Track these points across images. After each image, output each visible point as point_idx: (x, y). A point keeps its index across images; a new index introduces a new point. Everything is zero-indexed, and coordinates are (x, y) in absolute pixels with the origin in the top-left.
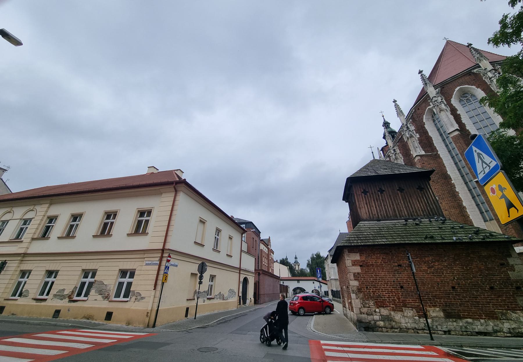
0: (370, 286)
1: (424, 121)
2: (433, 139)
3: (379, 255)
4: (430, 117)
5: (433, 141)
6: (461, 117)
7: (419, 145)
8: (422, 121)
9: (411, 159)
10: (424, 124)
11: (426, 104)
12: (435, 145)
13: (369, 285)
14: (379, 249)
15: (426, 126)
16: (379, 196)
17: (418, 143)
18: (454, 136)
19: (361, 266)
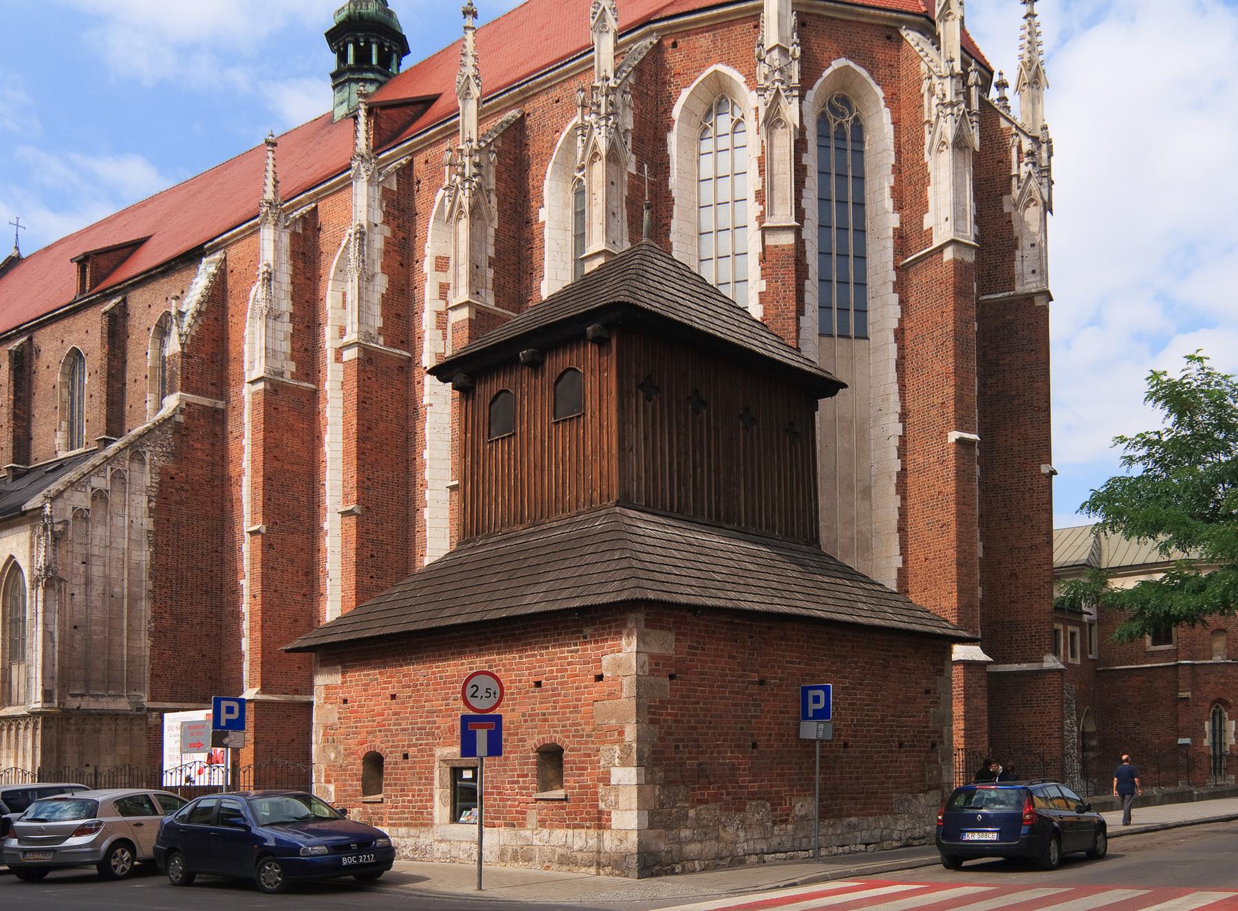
0: (686, 743)
1: (676, 112)
2: (675, 208)
3: (724, 645)
4: (701, 109)
5: (671, 217)
6: (804, 182)
7: (625, 211)
8: (669, 110)
9: (523, 243)
10: (669, 128)
11: (715, 46)
12: (673, 237)
13: (683, 740)
14: (726, 623)
15: (673, 139)
16: (687, 419)
17: (624, 198)
18: (776, 247)
19: (672, 677)
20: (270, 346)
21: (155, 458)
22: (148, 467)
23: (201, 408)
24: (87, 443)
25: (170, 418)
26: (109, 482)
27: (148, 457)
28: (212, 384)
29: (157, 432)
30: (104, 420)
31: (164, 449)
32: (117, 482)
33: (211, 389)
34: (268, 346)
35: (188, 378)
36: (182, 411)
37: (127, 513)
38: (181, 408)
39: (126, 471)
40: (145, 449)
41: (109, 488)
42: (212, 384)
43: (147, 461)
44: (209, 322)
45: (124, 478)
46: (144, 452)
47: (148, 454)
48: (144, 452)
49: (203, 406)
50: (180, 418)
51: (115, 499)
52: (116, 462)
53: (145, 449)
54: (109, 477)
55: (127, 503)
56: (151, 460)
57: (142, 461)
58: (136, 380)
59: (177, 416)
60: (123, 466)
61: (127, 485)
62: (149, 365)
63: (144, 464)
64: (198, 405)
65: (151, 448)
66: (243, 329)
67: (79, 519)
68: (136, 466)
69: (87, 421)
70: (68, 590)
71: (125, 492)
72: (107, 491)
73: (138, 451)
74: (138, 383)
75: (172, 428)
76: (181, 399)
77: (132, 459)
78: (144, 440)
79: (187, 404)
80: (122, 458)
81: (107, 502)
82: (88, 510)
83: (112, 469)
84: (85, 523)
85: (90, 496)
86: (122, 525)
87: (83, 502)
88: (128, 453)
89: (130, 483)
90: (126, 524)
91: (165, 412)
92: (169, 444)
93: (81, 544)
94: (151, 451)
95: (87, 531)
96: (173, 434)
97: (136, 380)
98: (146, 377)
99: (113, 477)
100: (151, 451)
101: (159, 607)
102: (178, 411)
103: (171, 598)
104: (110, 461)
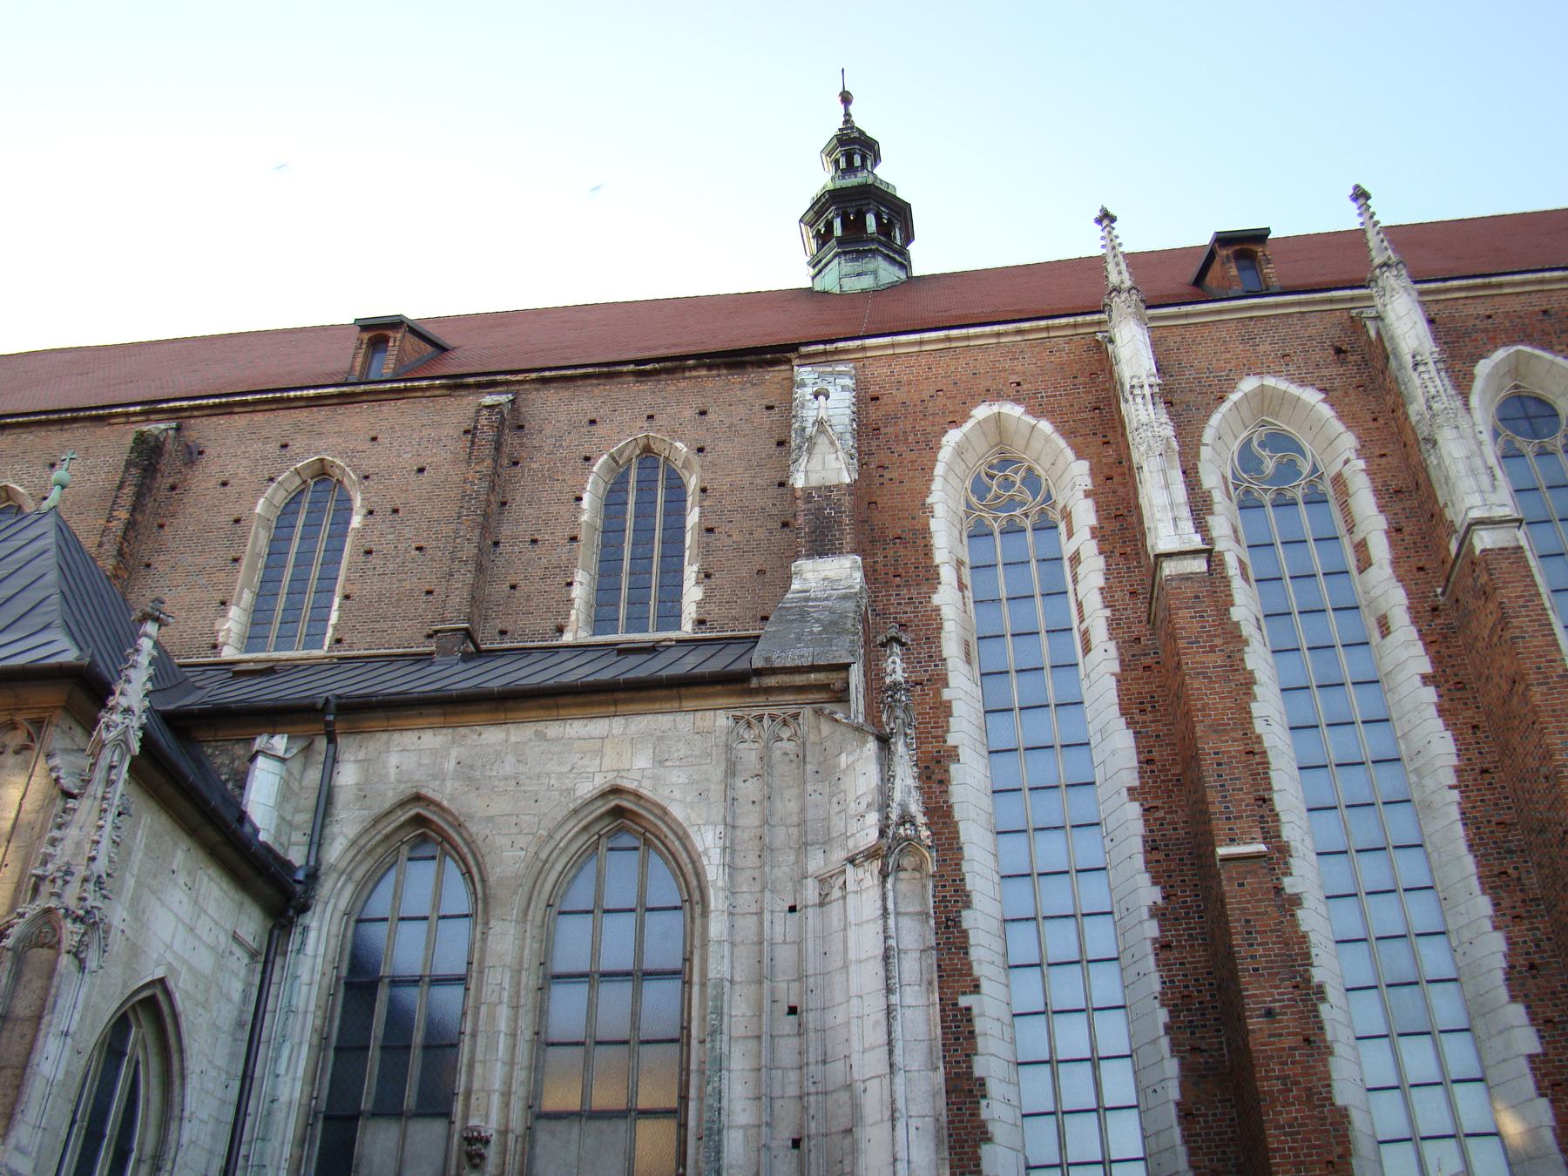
62: (584, 518)
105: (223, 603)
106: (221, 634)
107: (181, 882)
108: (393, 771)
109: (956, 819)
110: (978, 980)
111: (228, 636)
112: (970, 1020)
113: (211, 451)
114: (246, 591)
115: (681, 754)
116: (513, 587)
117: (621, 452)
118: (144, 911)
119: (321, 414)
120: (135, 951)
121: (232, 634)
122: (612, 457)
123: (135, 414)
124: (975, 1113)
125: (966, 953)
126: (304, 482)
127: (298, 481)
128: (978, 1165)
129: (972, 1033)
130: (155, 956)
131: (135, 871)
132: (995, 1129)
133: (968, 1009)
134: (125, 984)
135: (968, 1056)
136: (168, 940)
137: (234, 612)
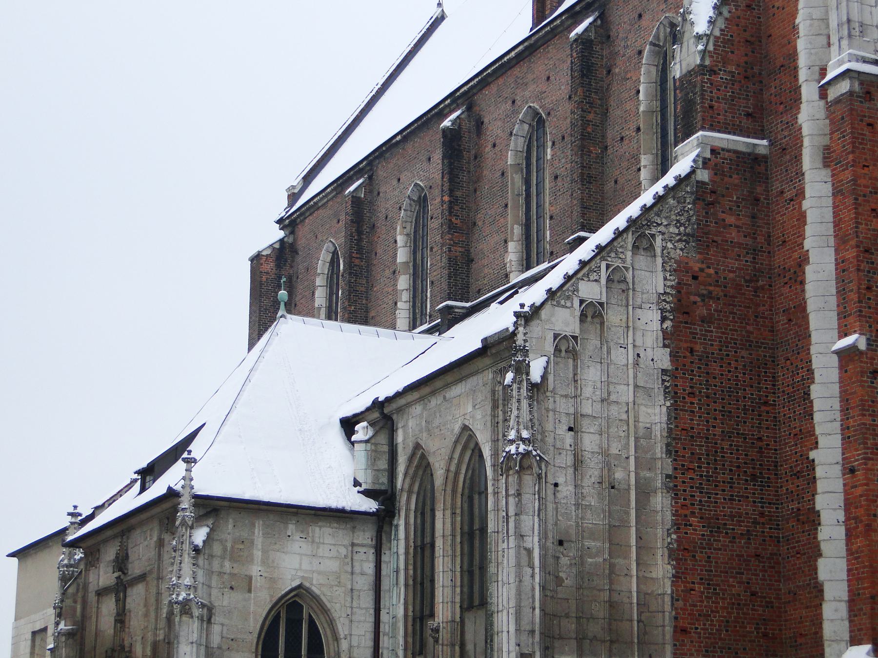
20: (855, 17)
21: (670, 245)
22: (659, 261)
23: (734, 156)
24: (552, 253)
25: (689, 176)
26: (604, 290)
27: (658, 242)
28: (748, 115)
29: (671, 201)
30: (577, 209)
31: (682, 229)
32: (617, 287)
33: (746, 123)
34: (851, 17)
35: (711, 107)
36: (706, 163)
37: (630, 340)
38: (705, 158)
39: (627, 269)
40: (654, 231)
41: (604, 300)
42: (748, 115)
43: (658, 251)
44: (739, 13)
45: (624, 281)
46: (653, 236)
47: (659, 239)
48: (653, 236)
49: (736, 152)
50: (703, 175)
51: (614, 317)
52: (613, 255)
53: (654, 231)
54: (603, 281)
55: (631, 324)
56: (664, 248)
57: (651, 248)
58: (622, 139)
59: (699, 172)
60: (624, 261)
61: (631, 292)
63: (655, 256)
64: (729, 151)
65: (660, 228)
66: (794, 14)
67: (563, 354)
68: (642, 260)
69: (551, 218)
70: (550, 477)
71: (627, 306)
72: (601, 304)
73: (643, 235)
74: (626, 142)
75: (692, 193)
76: (701, 144)
77: (636, 247)
78: (652, 214)
79: (713, 151)
80: (621, 247)
81: (602, 324)
82: (575, 338)
83: (608, 267)
84: (571, 361)
85: (578, 313)
86: (624, 362)
87: (567, 324)
88: (630, 238)
89: (634, 290)
90: (631, 361)
91: (681, 167)
92: (689, 220)
93: (566, 396)
94: (663, 234)
95: (575, 374)
96: (694, 203)
97: (622, 139)
98: (638, 129)
99: (609, 280)
100: (663, 234)
101: (683, 506)
102: (700, 163)
103: (700, 488)
104: (604, 254)
105: (506, 242)
106: (508, 265)
107: (298, 538)
108: (410, 430)
109: (808, 312)
110: (817, 438)
111: (511, 265)
112: (814, 469)
113: (486, 120)
114: (516, 226)
115: (479, 400)
116: (616, 182)
117: (657, 37)
118: (273, 562)
119: (524, 66)
120: (272, 581)
121: (513, 263)
122: (652, 44)
123: (449, 105)
124: (816, 538)
125: (812, 419)
126: (530, 125)
127: (526, 127)
128: (816, 574)
129: (815, 478)
130: (289, 577)
131: (260, 547)
132: (824, 547)
133: (813, 460)
134: (272, 596)
135: (813, 495)
136: (297, 566)
137: (511, 246)
